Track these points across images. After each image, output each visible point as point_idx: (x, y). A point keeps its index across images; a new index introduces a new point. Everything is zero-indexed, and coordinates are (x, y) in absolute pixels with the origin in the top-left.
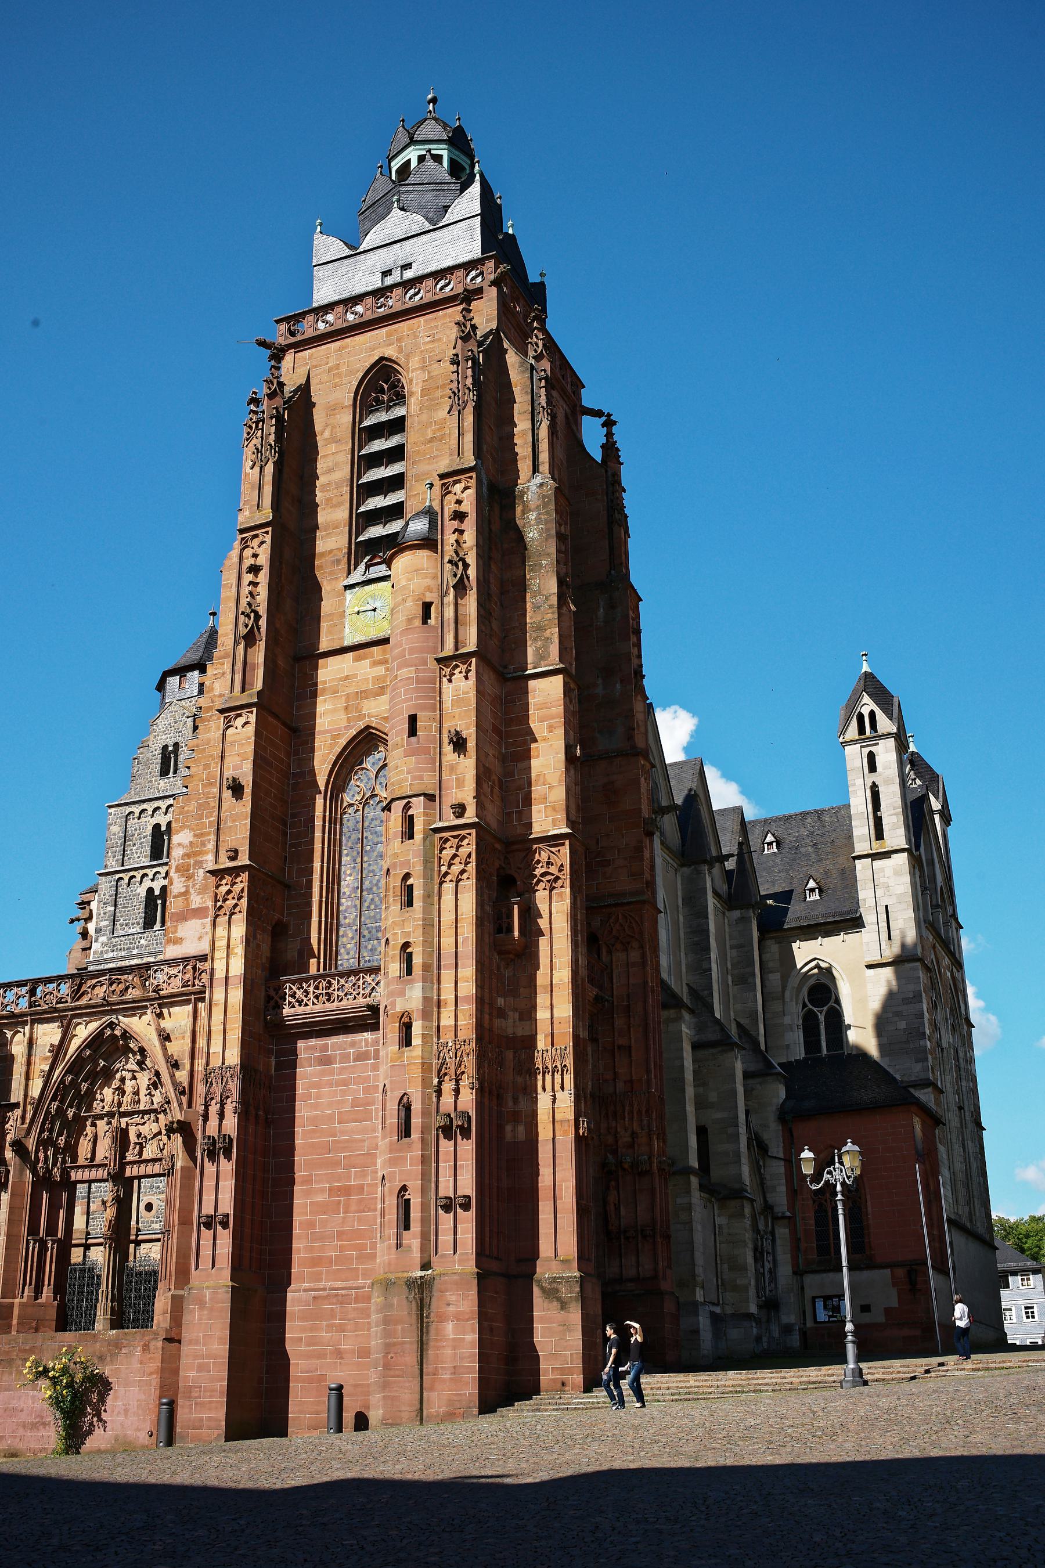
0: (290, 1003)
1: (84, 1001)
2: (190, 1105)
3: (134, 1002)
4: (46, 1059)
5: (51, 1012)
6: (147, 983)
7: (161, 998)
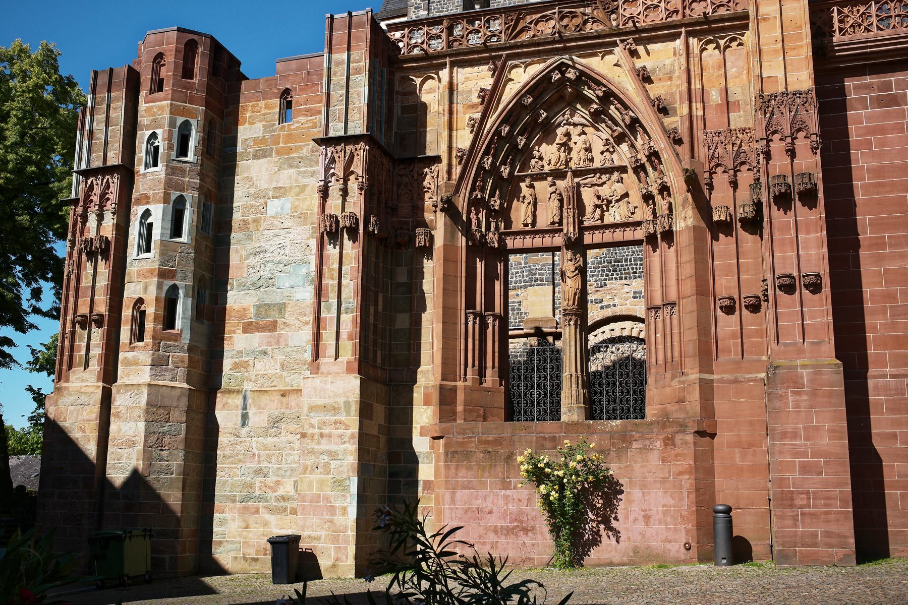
0: (841, 30)
1: (525, 37)
2: (693, 157)
3: (598, 37)
4: (473, 106)
5: (478, 52)
6: (613, 16)
7: (638, 31)
